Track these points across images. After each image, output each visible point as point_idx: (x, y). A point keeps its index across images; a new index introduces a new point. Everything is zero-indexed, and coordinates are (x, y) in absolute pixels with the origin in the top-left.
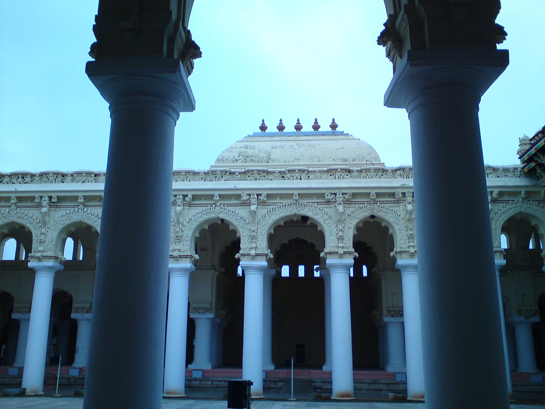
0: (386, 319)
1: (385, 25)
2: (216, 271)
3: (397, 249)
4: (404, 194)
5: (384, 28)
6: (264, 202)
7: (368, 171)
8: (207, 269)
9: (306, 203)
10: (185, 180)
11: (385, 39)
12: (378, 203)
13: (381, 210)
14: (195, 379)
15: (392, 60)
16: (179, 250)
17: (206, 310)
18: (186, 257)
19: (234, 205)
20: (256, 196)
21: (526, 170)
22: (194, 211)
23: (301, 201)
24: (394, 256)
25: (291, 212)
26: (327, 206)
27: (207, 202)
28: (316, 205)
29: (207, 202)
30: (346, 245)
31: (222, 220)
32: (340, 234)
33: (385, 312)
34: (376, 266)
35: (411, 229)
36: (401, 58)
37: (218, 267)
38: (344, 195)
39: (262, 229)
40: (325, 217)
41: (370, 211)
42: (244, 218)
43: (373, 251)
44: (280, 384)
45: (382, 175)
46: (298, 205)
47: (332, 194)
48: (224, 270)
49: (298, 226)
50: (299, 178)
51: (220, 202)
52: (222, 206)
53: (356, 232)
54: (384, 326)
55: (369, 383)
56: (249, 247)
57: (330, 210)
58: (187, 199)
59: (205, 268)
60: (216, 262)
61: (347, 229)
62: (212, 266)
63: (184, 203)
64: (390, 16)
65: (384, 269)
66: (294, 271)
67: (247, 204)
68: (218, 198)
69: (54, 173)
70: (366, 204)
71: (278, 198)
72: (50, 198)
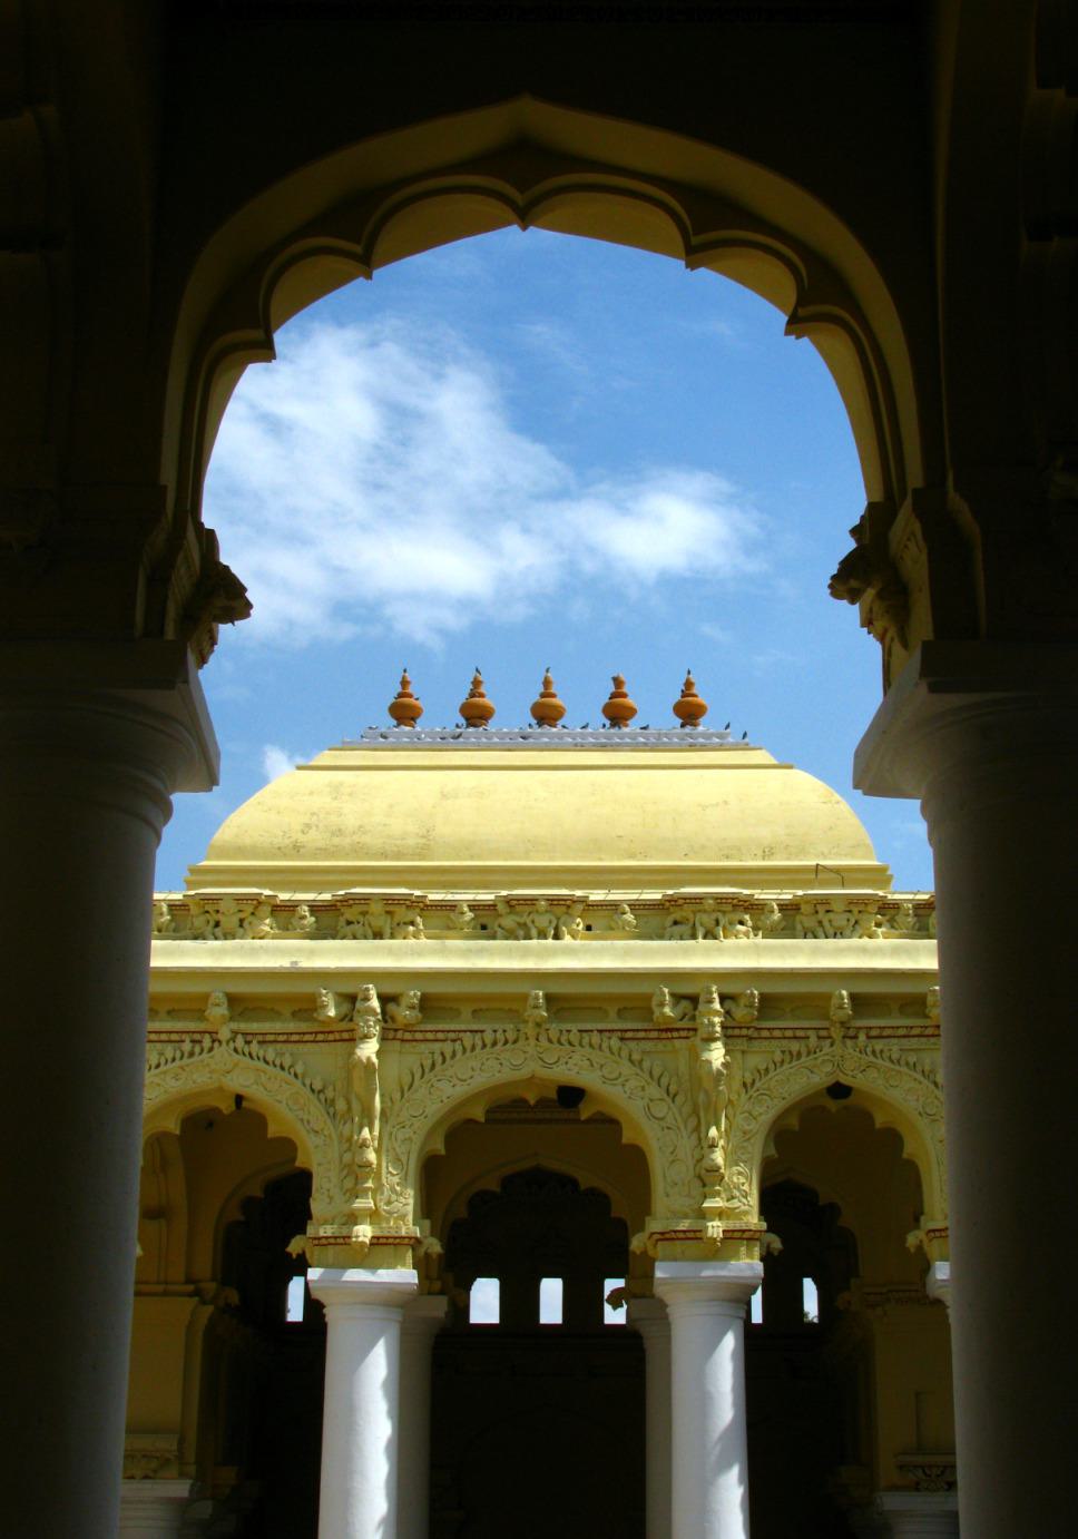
0: (890, 1502)
1: (855, 532)
2: (204, 1302)
5: (851, 545)
6: (408, 1028)
7: (821, 909)
8: (165, 1294)
9: (574, 1037)
11: (854, 583)
12: (862, 1037)
15: (882, 639)
23: (554, 1029)
24: (920, 1248)
25: (516, 1068)
26: (660, 1046)
27: (179, 1026)
28: (615, 1042)
29: (179, 1026)
30: (735, 1203)
31: (239, 1099)
36: (905, 645)
37: (210, 1287)
38: (728, 1003)
42: (330, 1093)
46: (543, 1038)
48: (234, 1297)
49: (540, 1121)
51: (234, 1026)
52: (240, 1040)
59: (160, 1288)
60: (205, 1265)
62: (189, 1281)
64: (871, 507)
66: (520, 1301)
68: (223, 1010)
70: (813, 1040)
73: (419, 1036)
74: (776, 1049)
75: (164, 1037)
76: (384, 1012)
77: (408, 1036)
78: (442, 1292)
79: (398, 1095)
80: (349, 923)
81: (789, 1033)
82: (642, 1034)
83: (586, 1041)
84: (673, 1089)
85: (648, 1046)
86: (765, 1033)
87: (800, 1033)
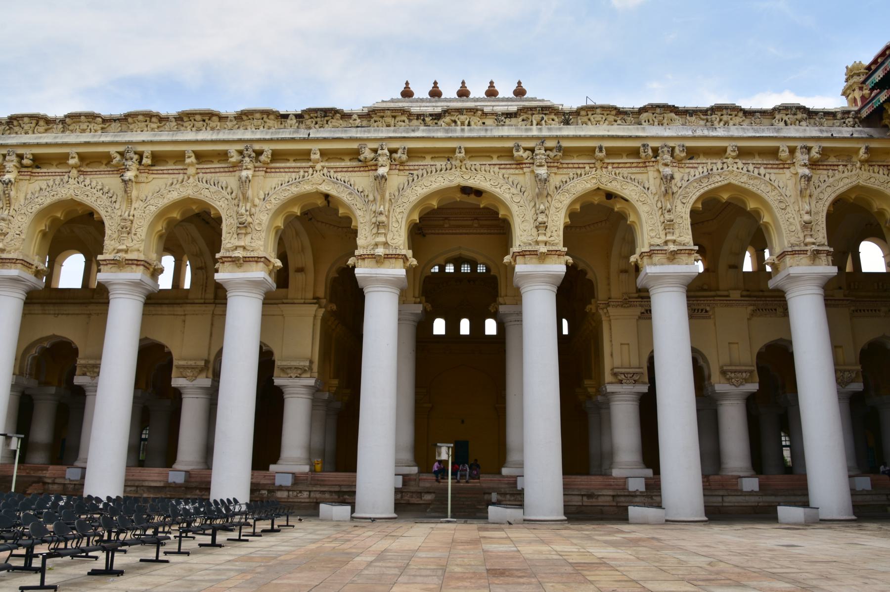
0: (610, 388)
2: (320, 307)
3: (643, 247)
4: (655, 151)
6: (402, 163)
7: (590, 113)
8: (304, 303)
9: (478, 167)
10: (261, 128)
12: (610, 167)
13: (615, 179)
14: (281, 488)
16: (244, 248)
17: (302, 372)
18: (257, 260)
19: (347, 170)
20: (386, 151)
21: (864, 113)
22: (273, 181)
23: (469, 163)
25: (450, 181)
26: (517, 171)
27: (298, 165)
30: (552, 239)
31: (327, 196)
32: (542, 218)
33: (608, 377)
34: (593, 301)
35: (669, 211)
37: (324, 301)
38: (548, 152)
39: (398, 210)
40: (513, 190)
41: (594, 181)
43: (588, 277)
44: (428, 497)
45: (616, 121)
47: (525, 149)
48: (334, 307)
49: (461, 234)
50: (467, 122)
51: (323, 164)
52: (325, 171)
53: (568, 220)
54: (607, 399)
55: (583, 495)
56: (373, 242)
57: (524, 179)
58: (263, 158)
59: (302, 301)
60: (321, 293)
61: (552, 210)
62: (314, 299)
63: (256, 165)
65: (608, 305)
66: (452, 327)
67: (370, 166)
68: (318, 156)
69: (31, 117)
71: (428, 157)
72: (21, 157)
73: (407, 168)
74: (571, 172)
75: (291, 170)
76: (391, 157)
77: (402, 168)
78: (420, 303)
79: (397, 194)
80: (375, 121)
81: (576, 166)
82: (508, 166)
83: (483, 169)
84: (523, 189)
85: (512, 171)
86: (565, 166)
87: (581, 166)
